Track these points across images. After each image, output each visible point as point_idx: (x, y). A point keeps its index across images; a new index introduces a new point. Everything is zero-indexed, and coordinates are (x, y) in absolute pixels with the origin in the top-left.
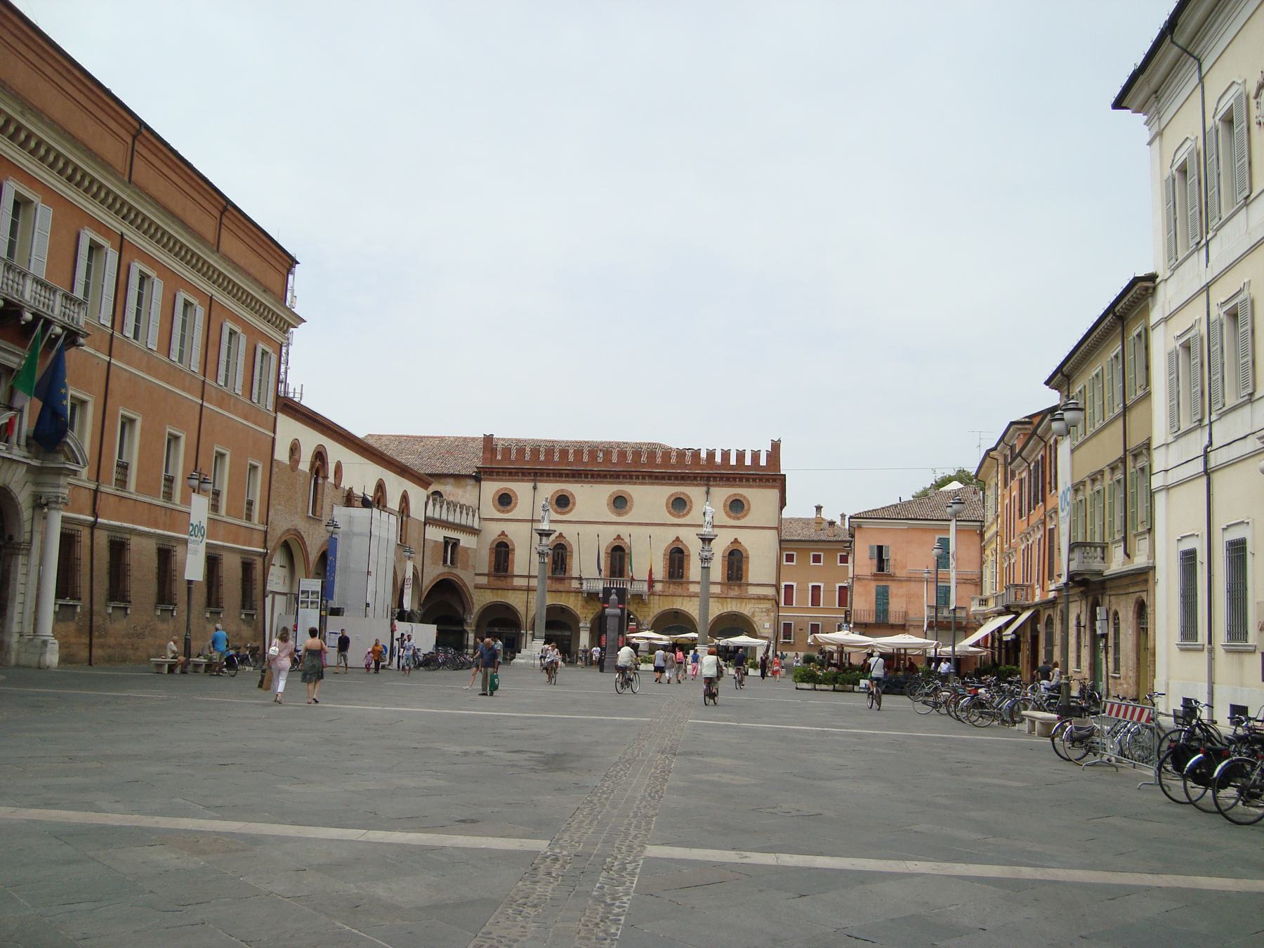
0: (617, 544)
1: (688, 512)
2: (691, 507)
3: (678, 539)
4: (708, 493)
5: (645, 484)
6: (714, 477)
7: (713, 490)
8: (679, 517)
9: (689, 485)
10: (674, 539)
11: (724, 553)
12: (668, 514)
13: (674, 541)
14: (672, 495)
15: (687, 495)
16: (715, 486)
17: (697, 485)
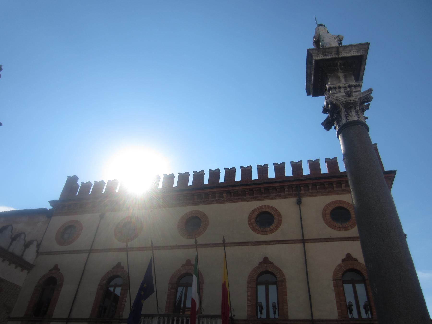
0: (185, 271)
1: (277, 227)
2: (281, 221)
3: (266, 260)
4: (299, 203)
5: (223, 202)
6: (306, 186)
7: (305, 200)
8: (265, 233)
9: (275, 198)
10: (262, 260)
11: (334, 275)
12: (251, 231)
13: (261, 263)
14: (255, 210)
15: (273, 208)
16: (307, 195)
17: (285, 197)
